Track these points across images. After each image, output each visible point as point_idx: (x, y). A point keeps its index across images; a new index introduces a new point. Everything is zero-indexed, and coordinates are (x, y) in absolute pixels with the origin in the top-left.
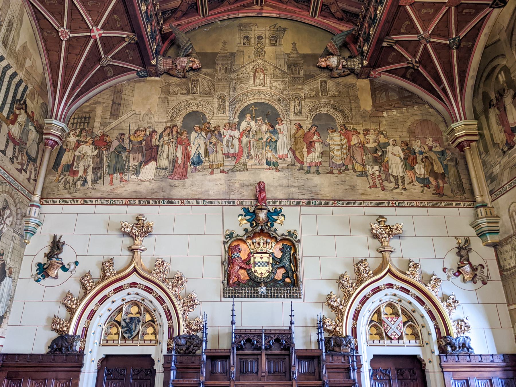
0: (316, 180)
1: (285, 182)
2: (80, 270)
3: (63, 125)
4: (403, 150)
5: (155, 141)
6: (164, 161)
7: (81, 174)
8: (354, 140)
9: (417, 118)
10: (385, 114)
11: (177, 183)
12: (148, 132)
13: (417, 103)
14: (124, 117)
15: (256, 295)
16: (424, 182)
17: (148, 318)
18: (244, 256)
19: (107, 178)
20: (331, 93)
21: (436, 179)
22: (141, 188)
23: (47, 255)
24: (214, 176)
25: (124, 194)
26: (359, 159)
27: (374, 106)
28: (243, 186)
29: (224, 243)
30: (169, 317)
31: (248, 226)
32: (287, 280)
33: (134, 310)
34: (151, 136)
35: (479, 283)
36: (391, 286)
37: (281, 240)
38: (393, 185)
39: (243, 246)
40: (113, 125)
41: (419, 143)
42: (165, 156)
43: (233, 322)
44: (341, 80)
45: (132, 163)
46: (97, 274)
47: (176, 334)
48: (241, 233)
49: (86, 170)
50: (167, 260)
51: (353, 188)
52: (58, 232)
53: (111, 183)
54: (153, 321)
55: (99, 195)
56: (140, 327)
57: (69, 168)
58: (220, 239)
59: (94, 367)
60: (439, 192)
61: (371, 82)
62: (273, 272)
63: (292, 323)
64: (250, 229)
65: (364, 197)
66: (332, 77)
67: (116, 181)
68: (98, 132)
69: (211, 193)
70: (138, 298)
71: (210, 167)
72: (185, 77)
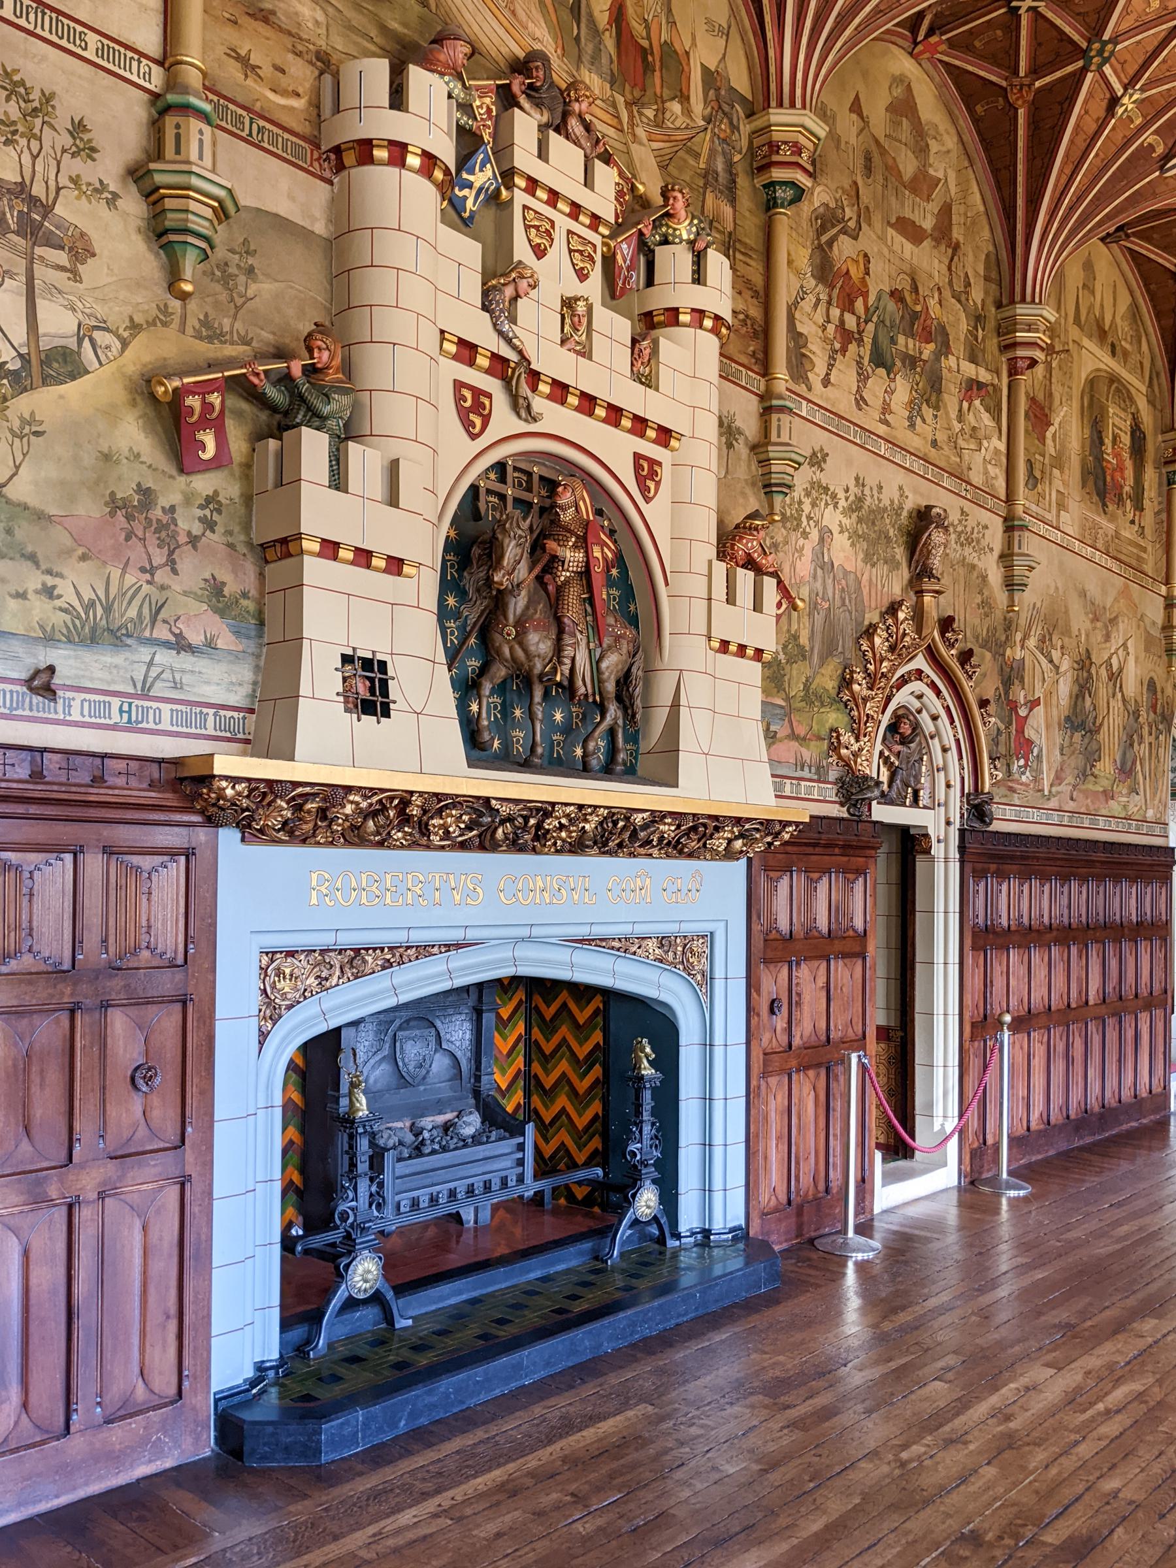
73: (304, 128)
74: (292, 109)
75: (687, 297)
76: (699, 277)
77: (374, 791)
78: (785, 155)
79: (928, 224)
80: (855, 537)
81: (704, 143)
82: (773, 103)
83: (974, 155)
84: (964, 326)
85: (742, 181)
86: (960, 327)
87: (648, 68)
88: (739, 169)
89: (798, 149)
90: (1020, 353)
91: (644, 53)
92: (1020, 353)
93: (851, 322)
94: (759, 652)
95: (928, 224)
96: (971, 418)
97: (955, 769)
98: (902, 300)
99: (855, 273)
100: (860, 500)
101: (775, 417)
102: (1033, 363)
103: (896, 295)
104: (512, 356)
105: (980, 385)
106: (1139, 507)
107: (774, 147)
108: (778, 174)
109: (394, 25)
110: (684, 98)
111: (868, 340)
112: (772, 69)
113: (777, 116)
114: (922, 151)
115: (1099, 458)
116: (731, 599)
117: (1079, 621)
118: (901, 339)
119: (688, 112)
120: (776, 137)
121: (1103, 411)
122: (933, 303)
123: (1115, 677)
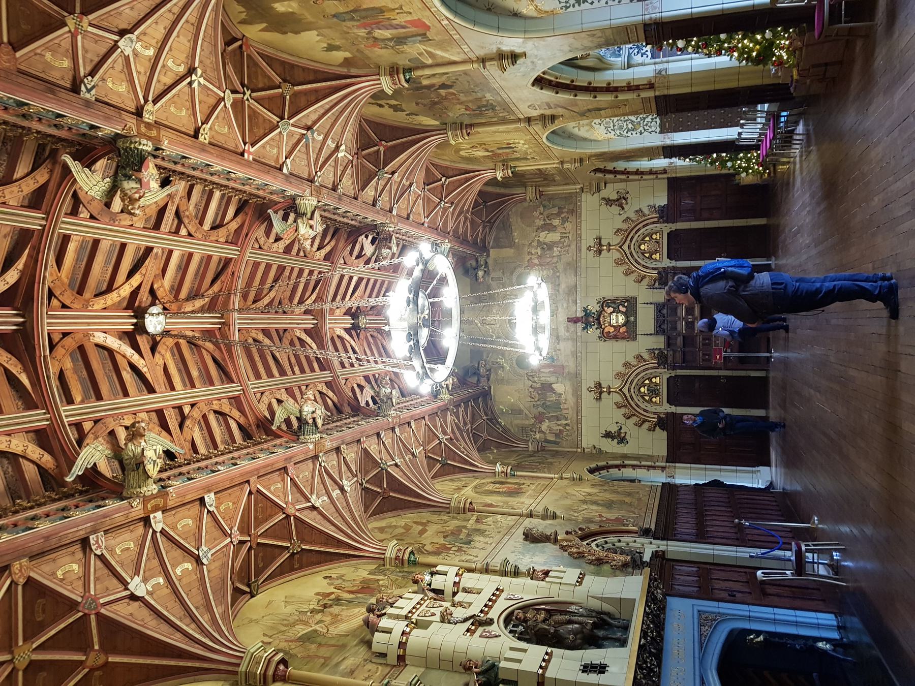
0: (563, 286)
1: (565, 305)
2: (622, 420)
3: (531, 441)
4: (542, 231)
5: (538, 386)
6: (552, 379)
7: (561, 428)
8: (536, 261)
9: (519, 220)
10: (517, 241)
11: (566, 370)
12: (532, 390)
13: (508, 219)
14: (521, 406)
15: (635, 323)
16: (565, 220)
17: (647, 382)
18: (612, 330)
19: (564, 412)
20: (501, 275)
21: (562, 213)
22: (570, 391)
23: (613, 440)
24: (562, 349)
25: (575, 400)
26: (550, 259)
27: (511, 247)
28: (568, 331)
29: (605, 341)
30: (647, 369)
31: (594, 327)
32: (626, 304)
33: (642, 390)
34: (534, 388)
35: (628, 195)
36: (629, 247)
37: (602, 307)
38: (567, 240)
39: (606, 330)
40: (527, 412)
41: (538, 220)
42: (548, 379)
43: (651, 334)
44: (490, 268)
45: (553, 398)
46: (624, 410)
47: (656, 365)
48: (599, 331)
49: (559, 425)
50: (614, 373)
51: (568, 264)
52: (599, 435)
53: (568, 409)
54: (648, 379)
55: (575, 415)
56: (652, 385)
57: (557, 435)
58: (602, 343)
59: (673, 407)
60: (572, 212)
61: (492, 248)
62: (622, 312)
63: (651, 303)
64: (596, 326)
65: (575, 258)
66: (489, 274)
67: (566, 406)
68: (533, 421)
69: (573, 350)
70: (637, 388)
71: (555, 351)
72: (490, 370)
73: (388, 669)
74: (382, 671)
75: (451, 578)
76: (445, 574)
77: (636, 670)
78: (400, 554)
79: (421, 528)
80: (534, 555)
81: (393, 577)
82: (383, 556)
83: (396, 514)
84: (456, 521)
85: (406, 570)
86: (455, 523)
87: (368, 587)
88: (402, 570)
89: (400, 550)
90: (467, 506)
91: (363, 587)
92: (467, 506)
93: (456, 549)
94: (581, 574)
95: (421, 528)
96: (489, 523)
97: (626, 539)
98: (447, 536)
99: (437, 546)
100: (520, 552)
101: (490, 567)
102: (471, 503)
103: (445, 537)
104: (471, 621)
105: (477, 519)
106: (523, 484)
107: (397, 558)
108: (406, 557)
109: (355, 643)
110: (378, 580)
111: (460, 545)
112: (372, 555)
113: (388, 555)
114: (396, 527)
115: (505, 492)
116: (562, 578)
117: (568, 502)
118: (461, 537)
119: (382, 580)
120: (393, 556)
121: (488, 490)
122: (447, 528)
123: (590, 494)
